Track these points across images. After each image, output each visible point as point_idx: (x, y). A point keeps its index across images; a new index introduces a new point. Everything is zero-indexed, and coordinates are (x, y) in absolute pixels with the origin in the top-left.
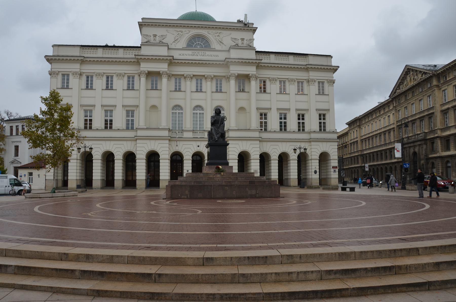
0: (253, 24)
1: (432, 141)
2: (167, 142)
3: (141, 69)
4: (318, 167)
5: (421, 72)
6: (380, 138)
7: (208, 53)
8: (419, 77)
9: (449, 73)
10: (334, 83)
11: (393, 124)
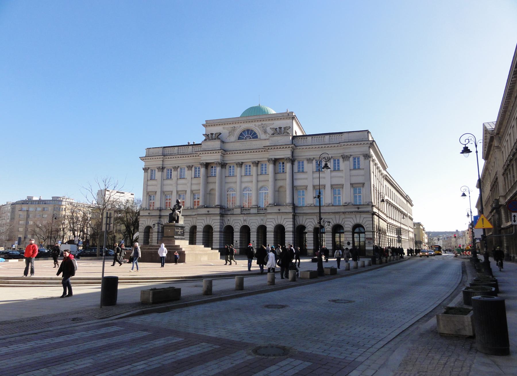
0: (293, 112)
3: (202, 162)
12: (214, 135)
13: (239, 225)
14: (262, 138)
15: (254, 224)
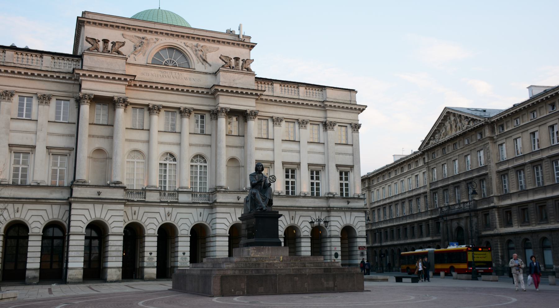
0: (250, 38)
1: (486, 212)
2: (122, 207)
4: (339, 249)
5: (467, 118)
6: (403, 207)
7: (185, 75)
8: (465, 126)
9: (507, 122)
10: (359, 128)
11: (425, 187)
12: (110, 45)
13: (157, 223)
14: (197, 70)
15: (184, 221)
